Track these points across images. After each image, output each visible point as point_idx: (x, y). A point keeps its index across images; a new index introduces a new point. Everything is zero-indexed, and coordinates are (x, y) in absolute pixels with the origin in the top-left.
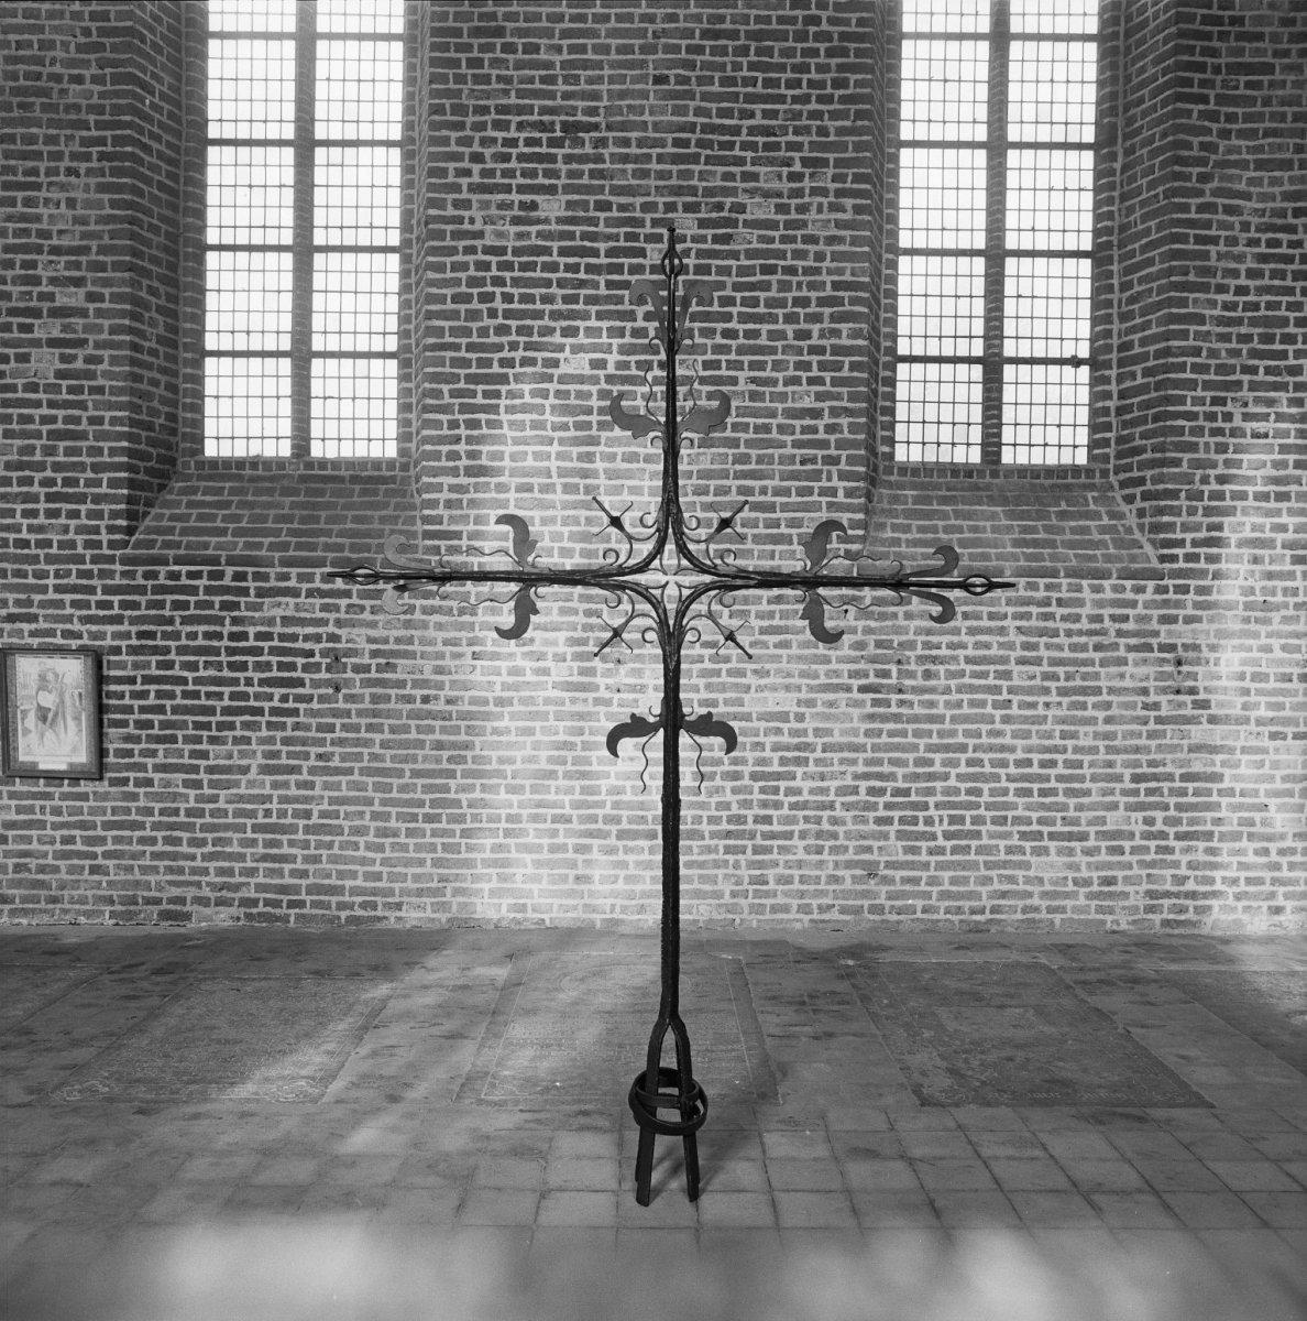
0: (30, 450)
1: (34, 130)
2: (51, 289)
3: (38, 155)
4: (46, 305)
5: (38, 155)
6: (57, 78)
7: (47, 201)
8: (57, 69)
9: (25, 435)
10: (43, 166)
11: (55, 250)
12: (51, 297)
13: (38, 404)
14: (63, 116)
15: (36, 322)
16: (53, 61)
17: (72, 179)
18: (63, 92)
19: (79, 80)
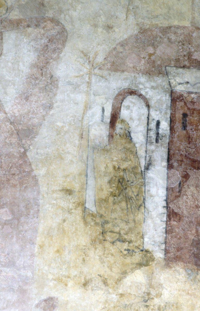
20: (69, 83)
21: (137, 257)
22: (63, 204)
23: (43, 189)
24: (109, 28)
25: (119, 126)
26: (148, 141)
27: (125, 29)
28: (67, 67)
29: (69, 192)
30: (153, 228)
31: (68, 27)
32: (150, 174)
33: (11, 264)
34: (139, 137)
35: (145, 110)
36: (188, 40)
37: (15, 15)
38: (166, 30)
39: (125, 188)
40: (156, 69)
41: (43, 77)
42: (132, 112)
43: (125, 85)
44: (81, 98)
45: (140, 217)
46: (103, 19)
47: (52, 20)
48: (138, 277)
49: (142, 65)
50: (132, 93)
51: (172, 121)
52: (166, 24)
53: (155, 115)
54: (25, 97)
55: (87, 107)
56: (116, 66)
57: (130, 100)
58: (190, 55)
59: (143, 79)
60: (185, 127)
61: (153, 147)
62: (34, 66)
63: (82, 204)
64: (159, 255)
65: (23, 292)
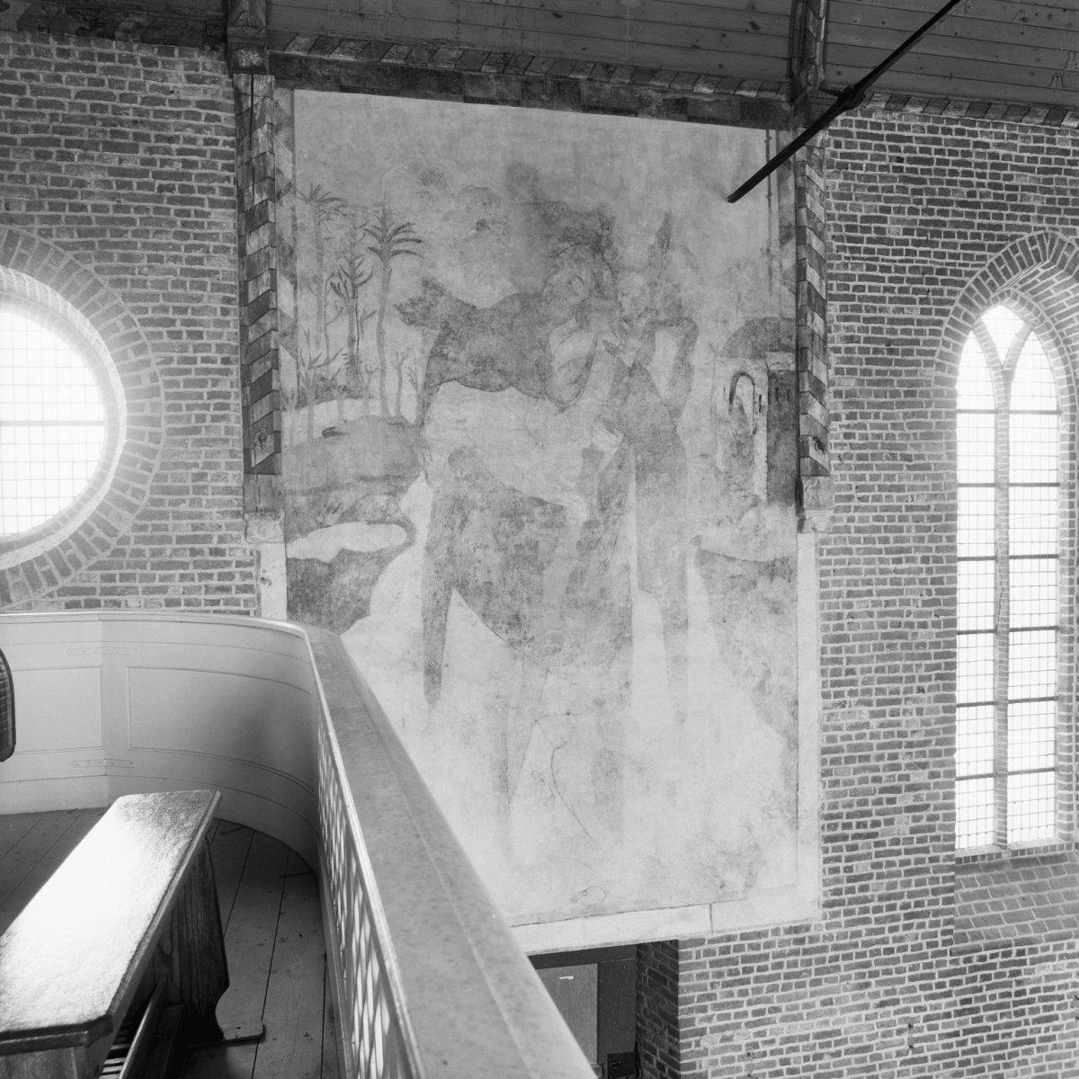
0: (893, 886)
1: (897, 662)
2: (907, 772)
3: (899, 680)
4: (903, 784)
5: (899, 680)
6: (910, 625)
7: (905, 711)
8: (911, 619)
9: (891, 875)
10: (902, 687)
11: (910, 745)
12: (907, 777)
13: (898, 853)
14: (914, 651)
15: (898, 796)
16: (909, 614)
17: (921, 695)
18: (915, 634)
19: (924, 625)
20: (701, 370)
21: (750, 501)
22: (702, 466)
23: (689, 455)
24: (725, 322)
25: (735, 401)
26: (754, 412)
27: (737, 324)
28: (699, 357)
29: (704, 456)
30: (759, 480)
31: (699, 324)
32: (757, 437)
33: (672, 513)
34: (748, 410)
35: (751, 387)
36: (777, 329)
37: (662, 317)
38: (763, 321)
39: (741, 448)
40: (758, 355)
41: (684, 367)
42: (744, 389)
43: (738, 368)
44: (709, 380)
45: (750, 471)
46: (720, 316)
47: (687, 319)
48: (751, 515)
49: (749, 351)
50: (743, 374)
51: (769, 395)
52: (763, 316)
53: (759, 391)
54: (673, 383)
55: (714, 388)
56: (731, 353)
57: (742, 379)
58: (779, 340)
59: (749, 363)
60: (777, 399)
61: (757, 416)
62: (677, 358)
63: (713, 464)
64: (764, 497)
65: (680, 533)
